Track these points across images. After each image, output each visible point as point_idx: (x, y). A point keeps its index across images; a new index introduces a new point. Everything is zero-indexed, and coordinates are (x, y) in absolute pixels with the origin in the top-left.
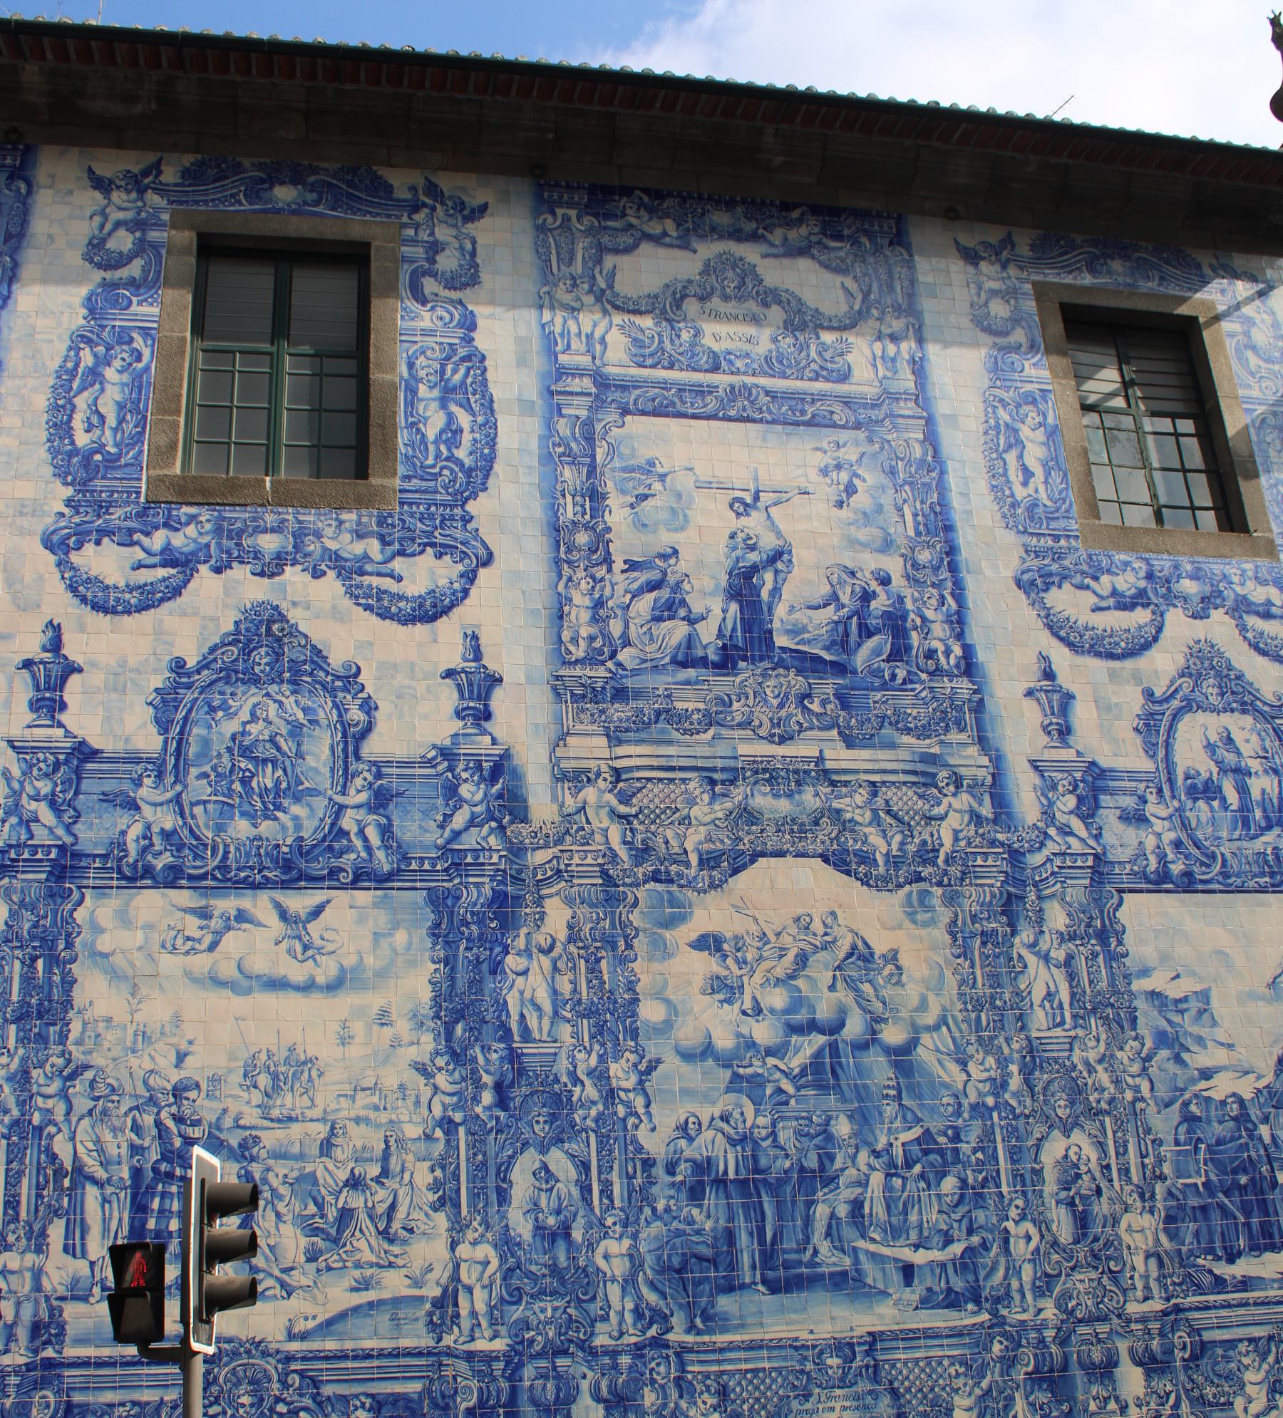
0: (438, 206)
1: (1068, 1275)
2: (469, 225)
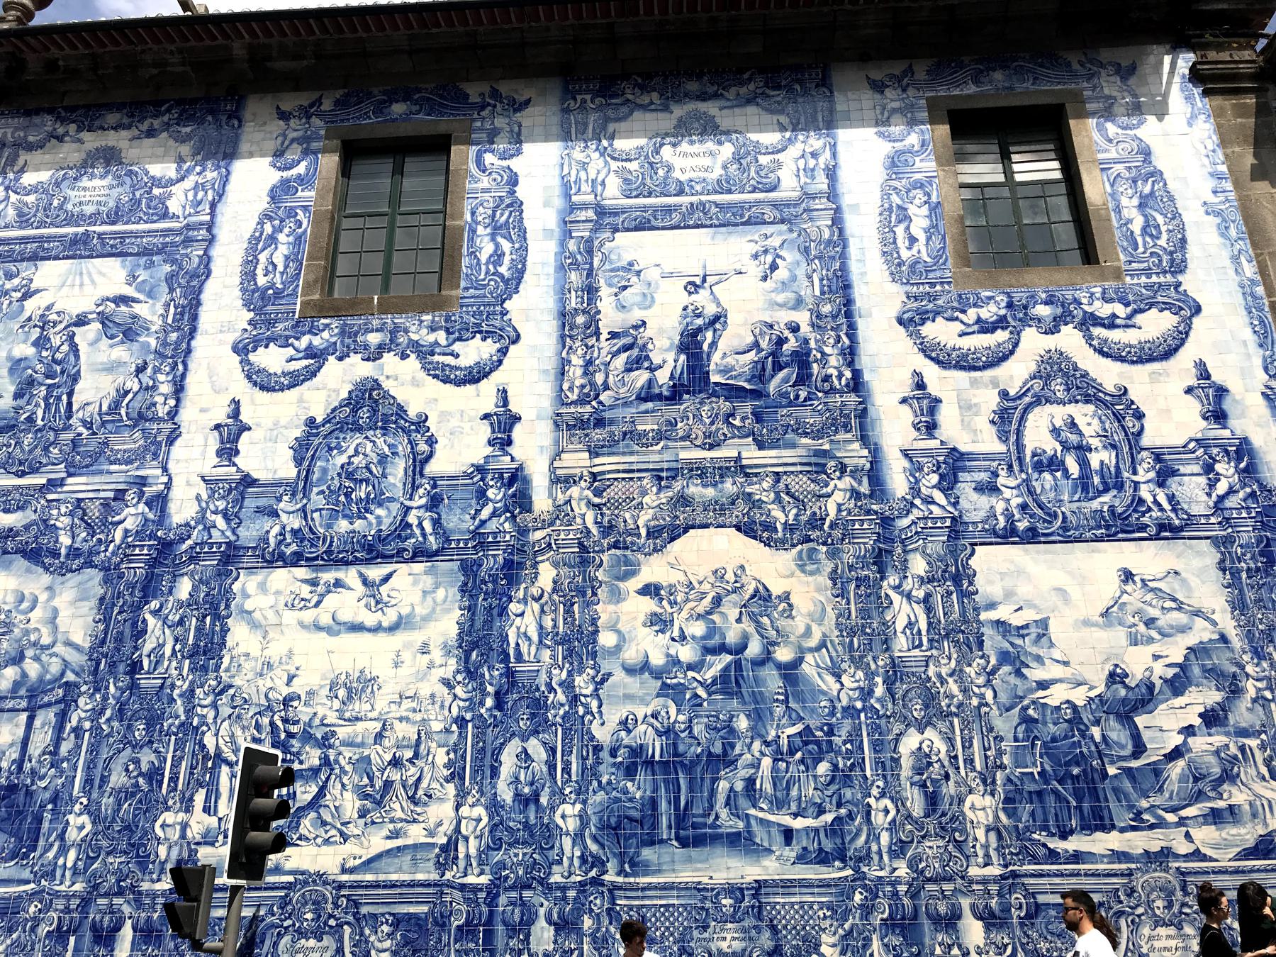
1: (919, 842)
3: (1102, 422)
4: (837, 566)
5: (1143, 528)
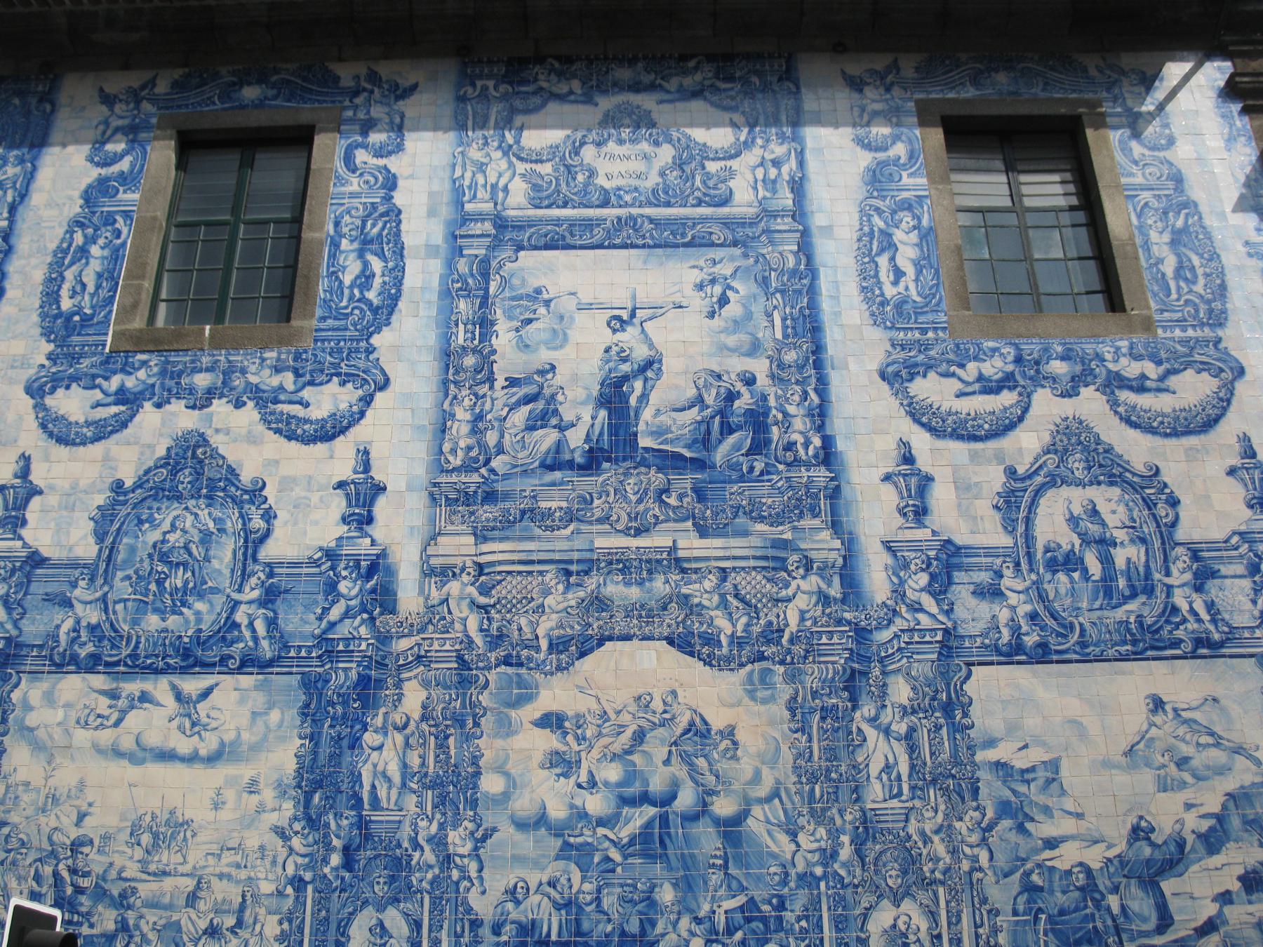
0: (376, 90)
2: (401, 103)
3: (1130, 510)
4: (797, 693)
5: (1176, 644)
